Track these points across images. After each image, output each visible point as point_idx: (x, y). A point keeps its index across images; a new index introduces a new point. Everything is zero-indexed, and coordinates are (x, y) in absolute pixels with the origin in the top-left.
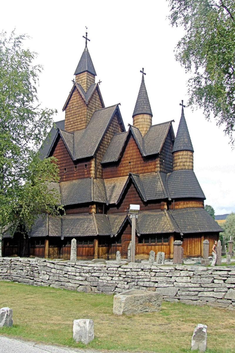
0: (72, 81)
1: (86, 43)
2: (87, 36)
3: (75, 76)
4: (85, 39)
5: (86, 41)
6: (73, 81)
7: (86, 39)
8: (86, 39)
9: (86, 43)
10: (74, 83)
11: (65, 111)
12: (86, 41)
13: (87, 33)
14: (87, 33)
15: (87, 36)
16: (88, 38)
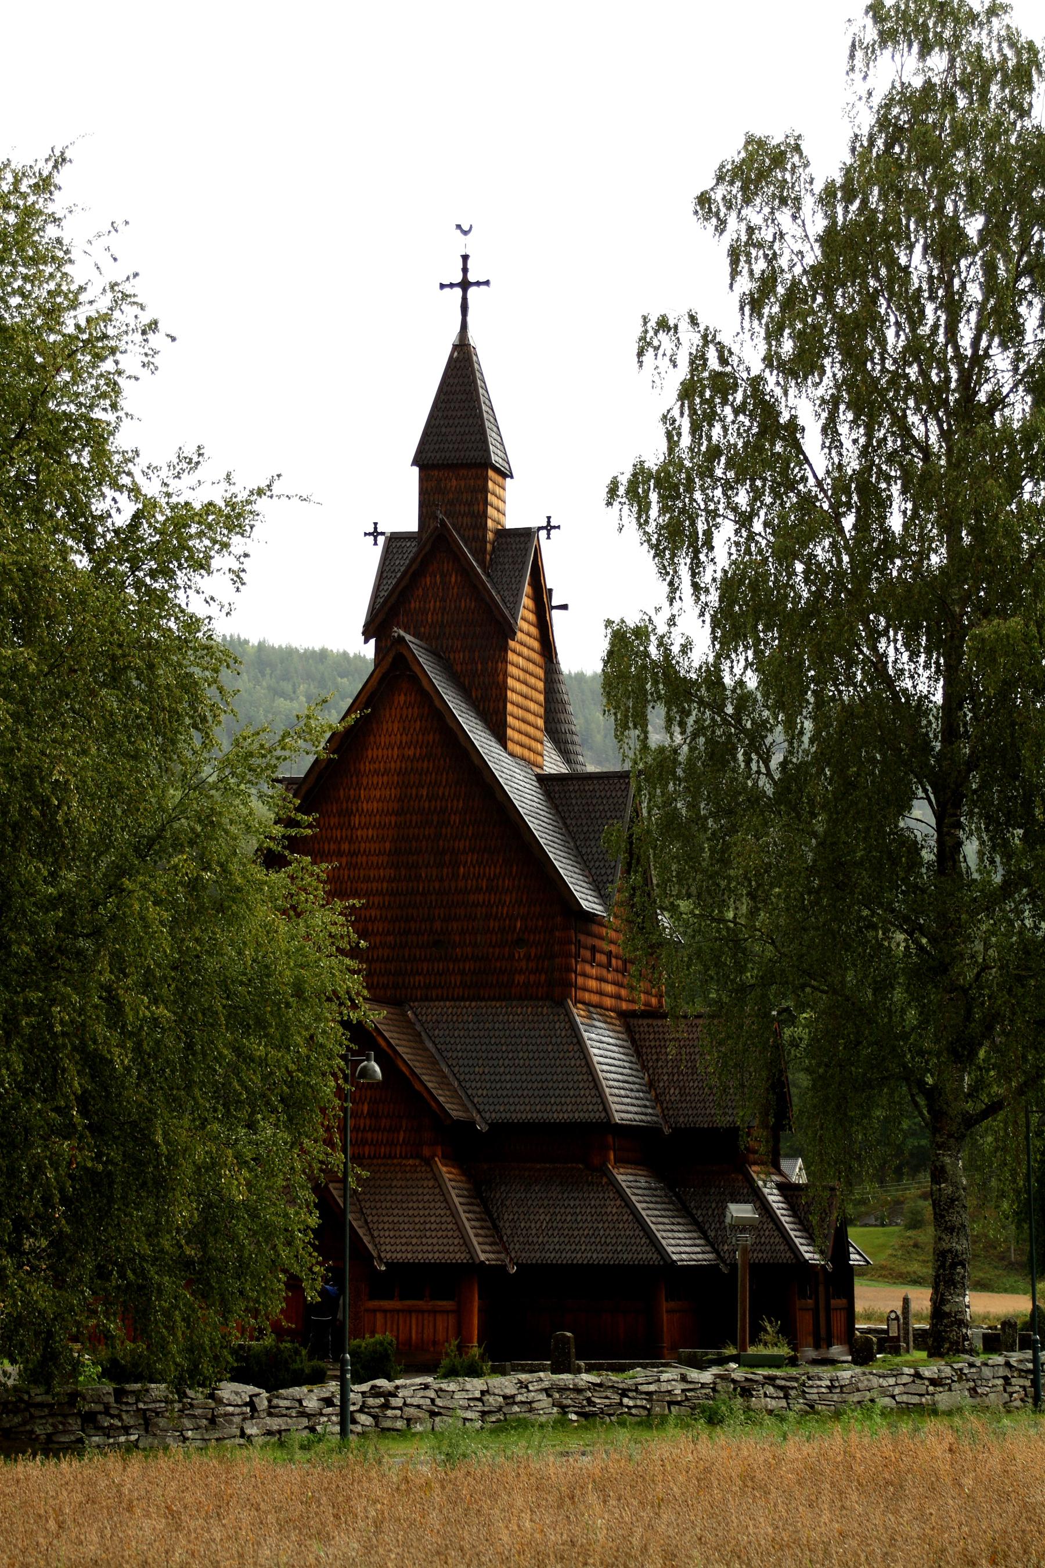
2: (465, 270)
6: (375, 534)
10: (381, 540)
13: (465, 258)
14: (465, 258)
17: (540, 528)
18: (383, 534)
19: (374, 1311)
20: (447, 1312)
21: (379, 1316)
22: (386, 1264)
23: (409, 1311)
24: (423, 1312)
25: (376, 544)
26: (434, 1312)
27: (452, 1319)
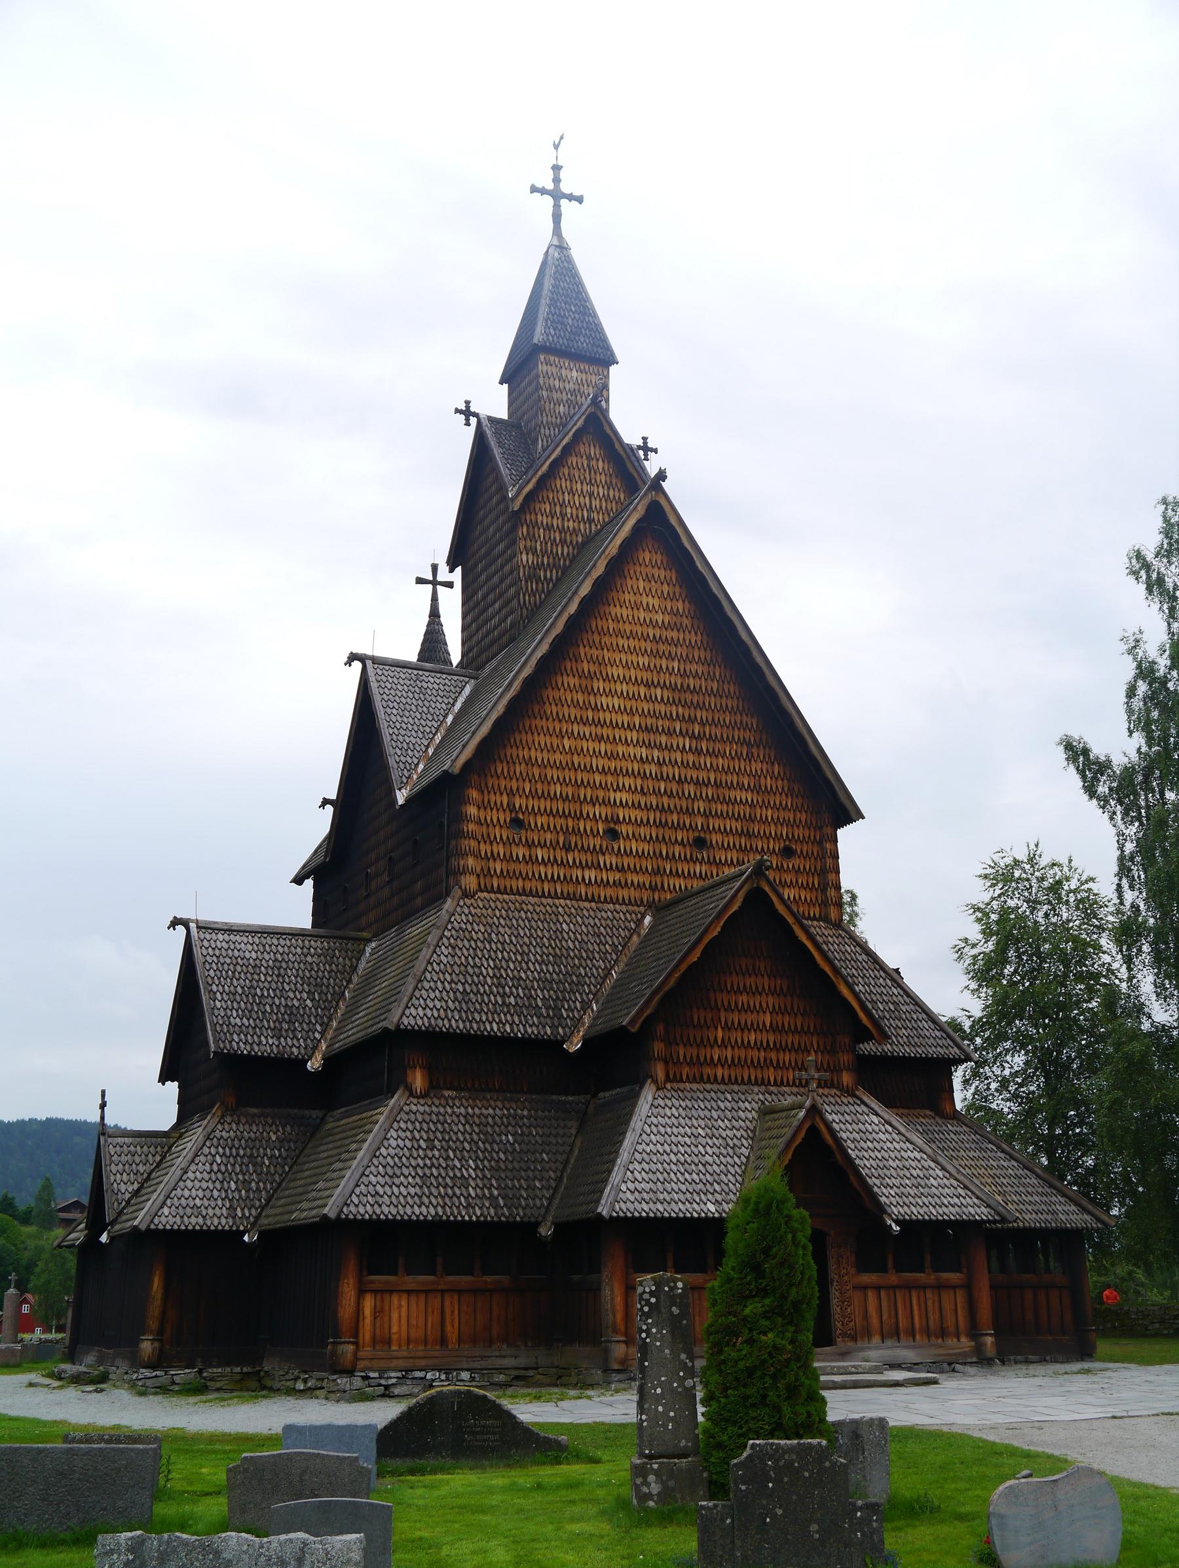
0: (457, 411)
1: (557, 217)
2: (557, 180)
3: (506, 386)
4: (549, 201)
5: (557, 206)
6: (467, 413)
7: (557, 195)
8: (557, 195)
9: (557, 217)
10: (473, 421)
11: (459, 570)
12: (557, 206)
13: (557, 168)
14: (557, 168)
15: (557, 180)
16: (565, 188)
17: (639, 447)
18: (476, 415)
19: (864, 1288)
20: (954, 1287)
21: (871, 1295)
22: (897, 1222)
23: (908, 1287)
24: (924, 1287)
25: (468, 424)
26: (939, 1287)
27: (960, 1296)
